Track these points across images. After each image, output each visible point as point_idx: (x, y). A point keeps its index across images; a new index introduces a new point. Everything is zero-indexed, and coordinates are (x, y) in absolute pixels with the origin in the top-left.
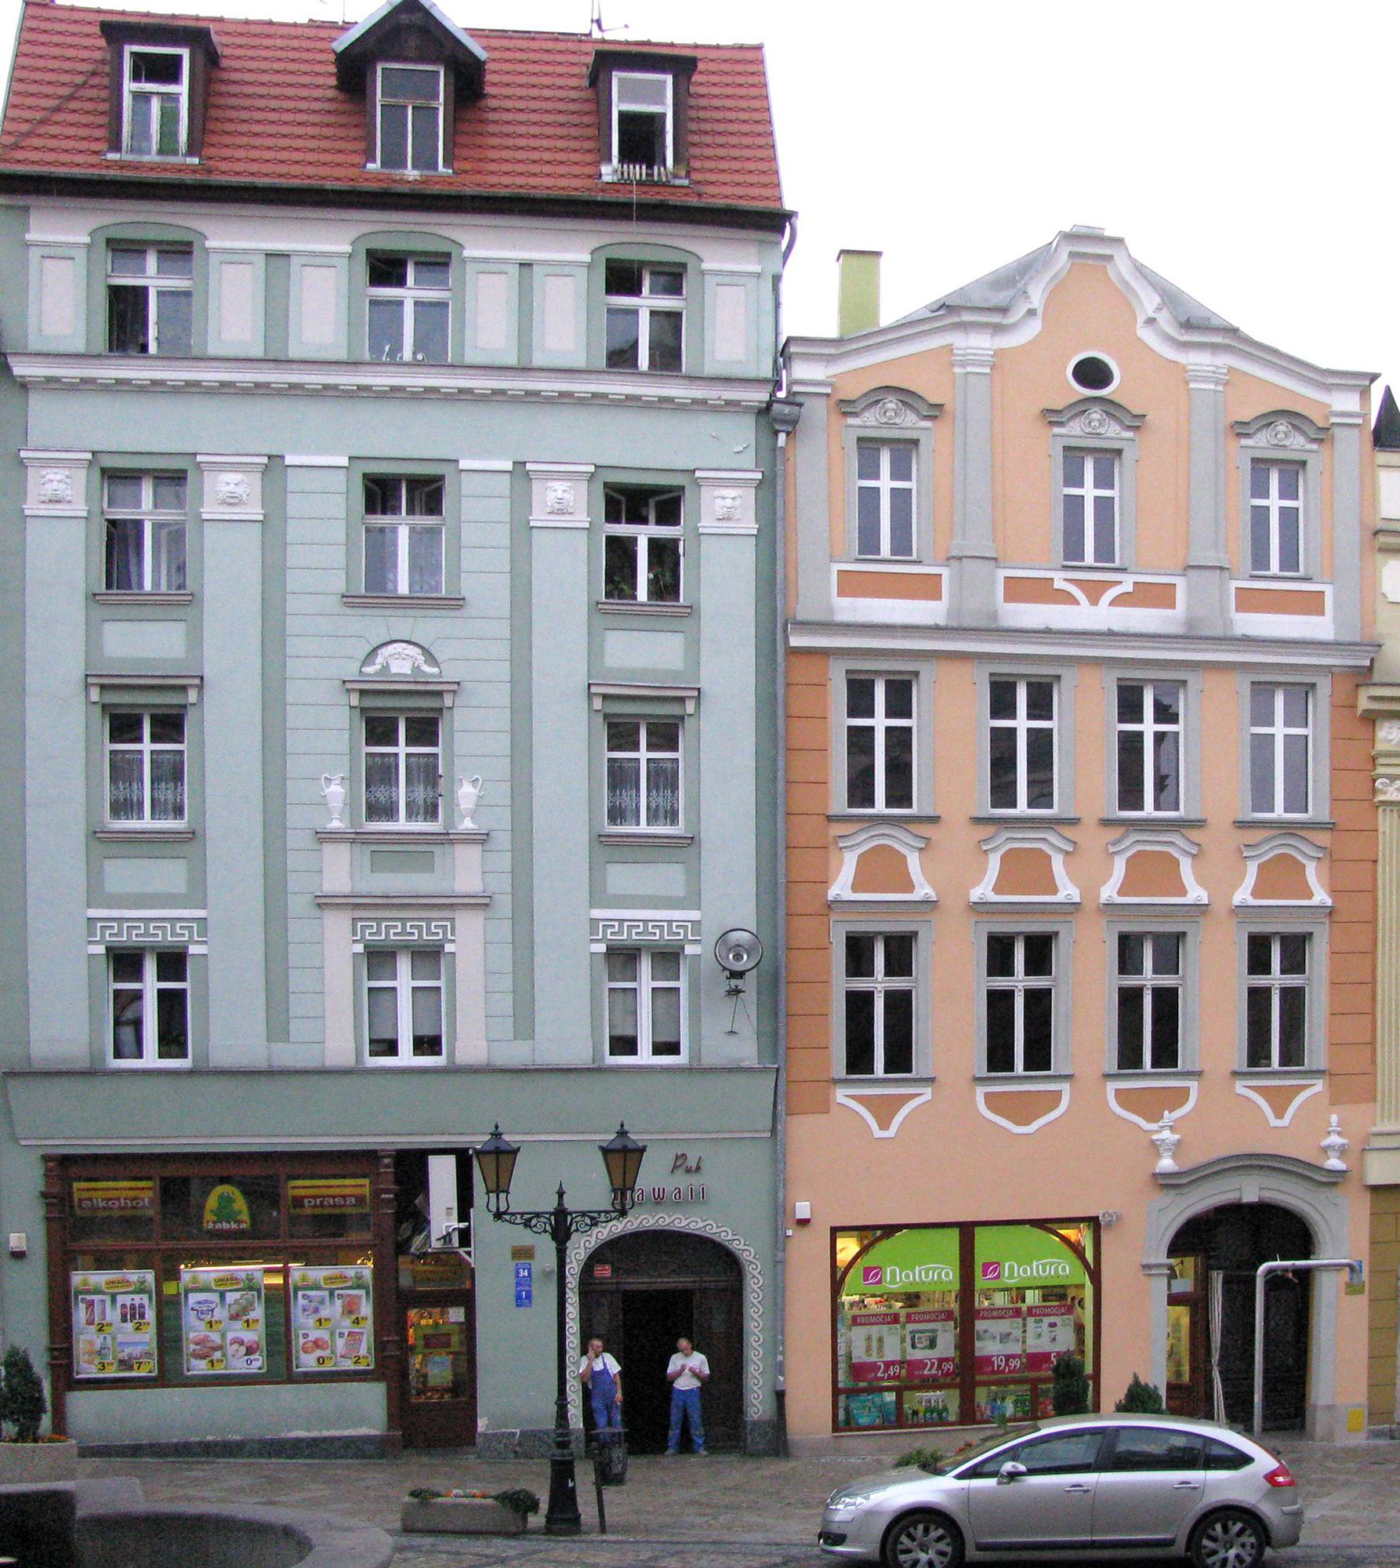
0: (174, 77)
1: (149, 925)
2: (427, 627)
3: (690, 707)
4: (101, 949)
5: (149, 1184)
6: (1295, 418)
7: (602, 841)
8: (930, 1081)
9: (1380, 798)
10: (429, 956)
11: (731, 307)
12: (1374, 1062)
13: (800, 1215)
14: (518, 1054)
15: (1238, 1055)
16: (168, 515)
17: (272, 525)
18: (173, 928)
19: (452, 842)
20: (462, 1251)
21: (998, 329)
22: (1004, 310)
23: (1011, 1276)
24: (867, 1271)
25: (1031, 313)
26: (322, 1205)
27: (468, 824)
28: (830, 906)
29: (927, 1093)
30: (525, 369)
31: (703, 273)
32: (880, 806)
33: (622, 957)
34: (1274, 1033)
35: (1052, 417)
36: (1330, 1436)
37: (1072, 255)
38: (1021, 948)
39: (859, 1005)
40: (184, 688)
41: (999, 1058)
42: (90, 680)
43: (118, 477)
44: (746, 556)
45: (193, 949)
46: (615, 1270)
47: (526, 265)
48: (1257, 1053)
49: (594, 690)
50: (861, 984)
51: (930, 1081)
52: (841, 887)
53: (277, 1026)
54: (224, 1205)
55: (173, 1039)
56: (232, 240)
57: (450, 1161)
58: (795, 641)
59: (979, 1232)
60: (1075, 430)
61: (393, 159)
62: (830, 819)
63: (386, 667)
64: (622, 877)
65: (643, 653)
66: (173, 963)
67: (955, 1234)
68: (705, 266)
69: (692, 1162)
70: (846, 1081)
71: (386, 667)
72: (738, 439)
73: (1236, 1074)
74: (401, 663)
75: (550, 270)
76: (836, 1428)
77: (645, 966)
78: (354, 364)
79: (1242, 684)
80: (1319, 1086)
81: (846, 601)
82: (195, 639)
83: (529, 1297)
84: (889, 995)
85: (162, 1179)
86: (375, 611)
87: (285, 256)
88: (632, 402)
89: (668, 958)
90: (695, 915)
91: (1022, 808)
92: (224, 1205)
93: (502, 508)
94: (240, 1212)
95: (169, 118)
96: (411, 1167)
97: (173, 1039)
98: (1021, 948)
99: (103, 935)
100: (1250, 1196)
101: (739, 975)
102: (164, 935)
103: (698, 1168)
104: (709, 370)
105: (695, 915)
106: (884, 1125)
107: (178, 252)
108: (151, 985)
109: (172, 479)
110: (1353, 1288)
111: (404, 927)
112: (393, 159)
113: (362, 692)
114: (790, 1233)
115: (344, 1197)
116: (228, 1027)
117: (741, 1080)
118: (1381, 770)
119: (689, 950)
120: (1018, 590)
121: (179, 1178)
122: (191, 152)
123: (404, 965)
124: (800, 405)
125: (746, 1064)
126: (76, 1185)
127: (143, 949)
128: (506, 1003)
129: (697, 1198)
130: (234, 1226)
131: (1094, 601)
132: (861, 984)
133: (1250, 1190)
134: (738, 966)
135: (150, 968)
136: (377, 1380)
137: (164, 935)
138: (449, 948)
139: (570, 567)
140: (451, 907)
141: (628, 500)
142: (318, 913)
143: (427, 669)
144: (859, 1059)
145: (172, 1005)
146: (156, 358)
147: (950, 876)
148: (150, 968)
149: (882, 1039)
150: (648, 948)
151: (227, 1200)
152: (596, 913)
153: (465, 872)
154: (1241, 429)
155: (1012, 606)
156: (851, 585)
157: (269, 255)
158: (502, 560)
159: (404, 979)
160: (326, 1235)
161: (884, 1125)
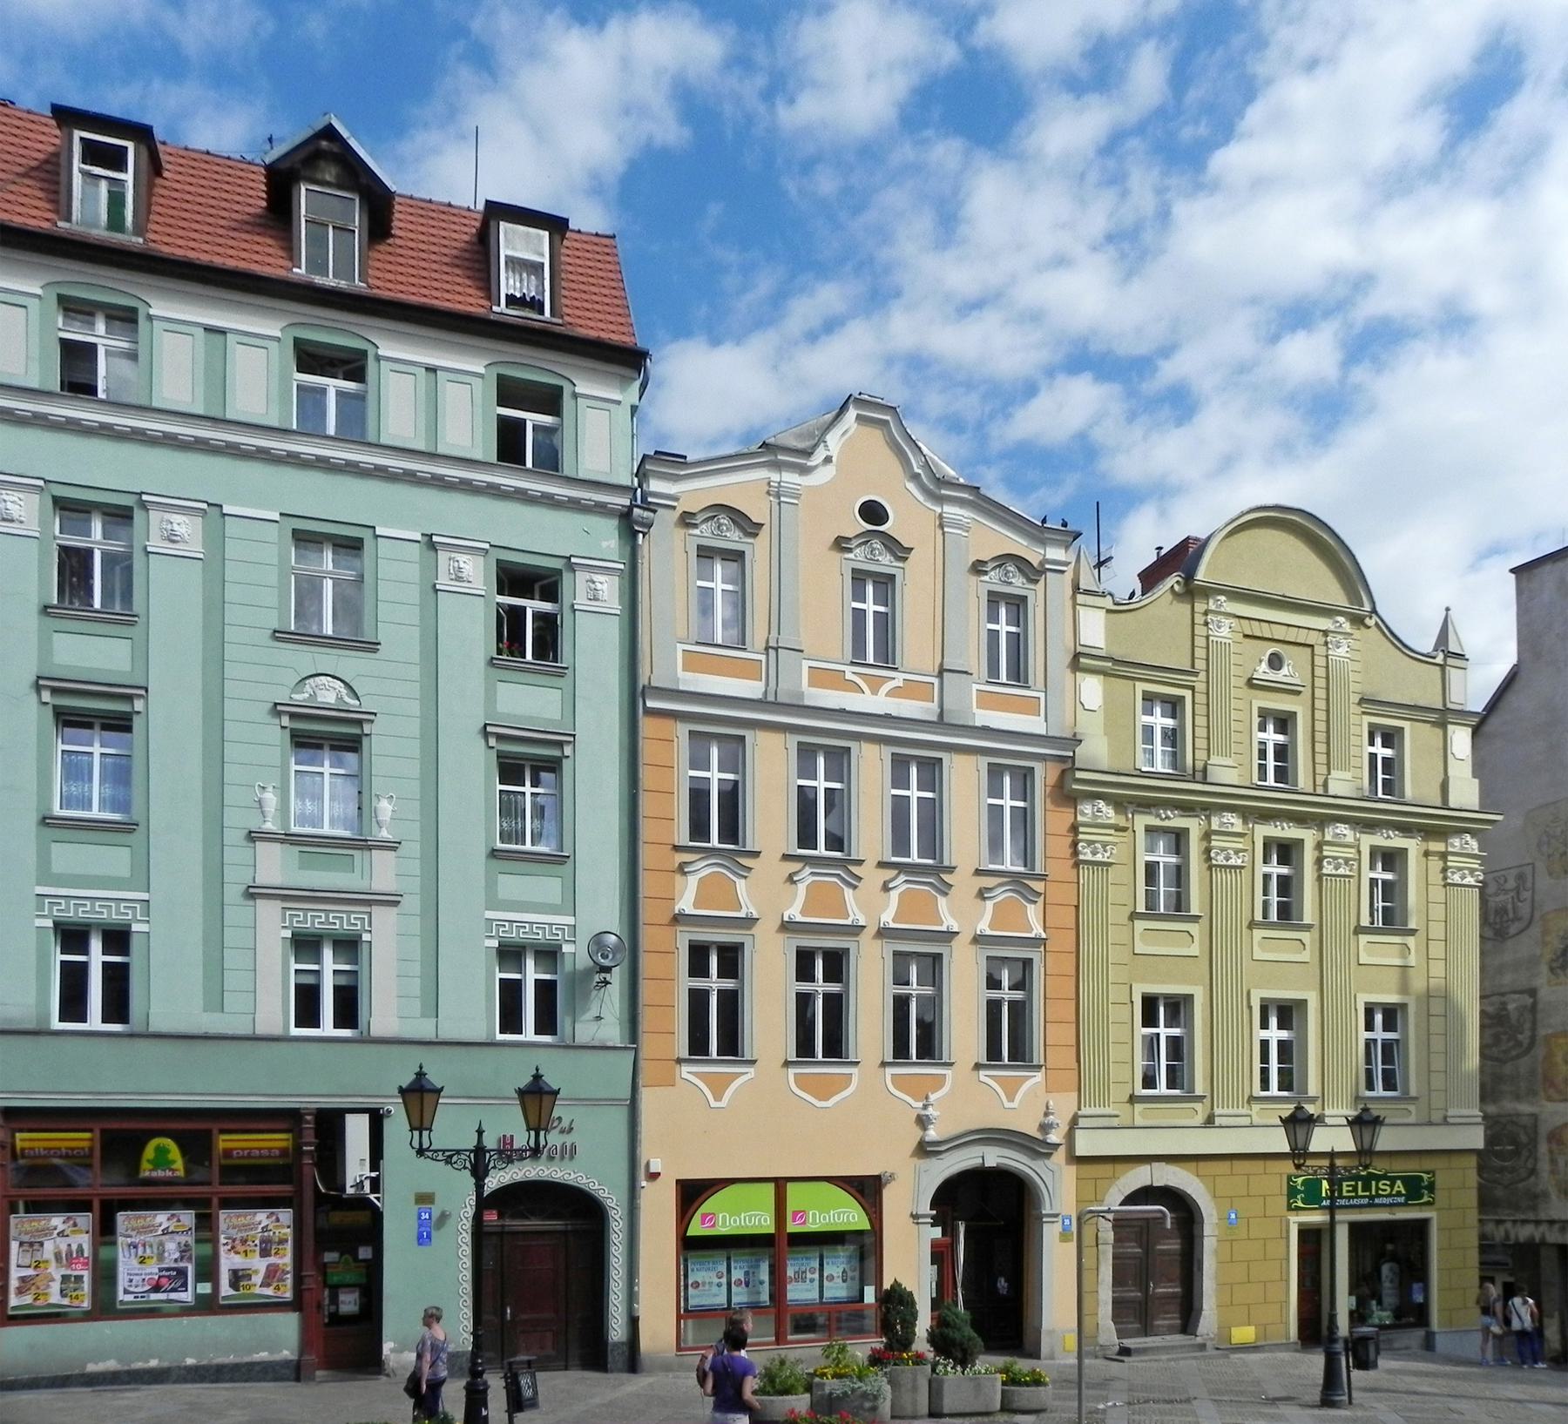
0: (120, 165)
1: (97, 905)
2: (350, 664)
3: (568, 750)
4: (49, 923)
5: (87, 1135)
6: (1021, 563)
7: (494, 854)
8: (753, 1062)
9: (1081, 857)
10: (349, 946)
11: (600, 429)
12: (1079, 1061)
13: (652, 1170)
14: (425, 1030)
15: (979, 1051)
16: (116, 546)
17: (214, 562)
18: (118, 908)
19: (370, 848)
20: (372, 1197)
21: (805, 470)
22: (808, 453)
23: (814, 1222)
24: (704, 1216)
25: (828, 460)
26: (249, 1156)
27: (384, 834)
28: (679, 919)
29: (751, 1070)
30: (433, 456)
31: (575, 396)
32: (715, 841)
33: (510, 954)
34: (1009, 1039)
35: (841, 544)
36: (1052, 1357)
37: (859, 417)
38: (823, 962)
39: (698, 1000)
40: (129, 698)
41: (805, 1047)
42: (41, 682)
43: (71, 509)
44: (613, 632)
45: (135, 927)
46: (501, 1216)
47: (432, 370)
48: (993, 1052)
49: (489, 729)
50: (699, 983)
51: (753, 1062)
52: (686, 904)
53: (216, 999)
54: (164, 1157)
55: (117, 1007)
56: (174, 315)
57: (364, 1119)
58: (650, 704)
59: (790, 1186)
60: (859, 557)
61: (318, 265)
62: (677, 848)
63: (313, 696)
64: (513, 885)
65: (529, 702)
66: (117, 939)
67: (771, 1187)
68: (577, 390)
69: (565, 1124)
70: (685, 1061)
71: (313, 696)
72: (605, 538)
73: (978, 1066)
74: (329, 694)
75: (452, 376)
76: (679, 1348)
77: (530, 963)
78: (284, 432)
79: (983, 762)
80: (1039, 1077)
81: (689, 675)
82: (142, 655)
83: (429, 1237)
84: (722, 993)
85: (103, 1131)
86: (305, 648)
87: (222, 332)
88: (521, 496)
89: (549, 955)
90: (570, 920)
91: (821, 850)
92: (164, 1157)
93: (413, 572)
94: (174, 1162)
95: (116, 201)
96: (330, 1124)
97: (117, 1007)
98: (823, 962)
99: (51, 910)
100: (991, 1162)
101: (607, 970)
102: (110, 913)
103: (571, 1129)
104: (581, 476)
105: (570, 920)
106: (718, 1098)
107: (124, 318)
108: (96, 957)
109: (119, 516)
110: (1064, 1236)
111: (327, 917)
112: (318, 265)
113: (293, 716)
114: (644, 1183)
115: (270, 1149)
116: (166, 997)
117: (610, 1055)
118: (1081, 837)
119: (566, 948)
120: (821, 678)
121: (123, 1132)
122: (139, 230)
123: (328, 953)
124: (654, 512)
125: (610, 1044)
126: (18, 1135)
127: (88, 925)
128: (415, 986)
129: (569, 1153)
130: (169, 1174)
131: (875, 692)
132: (699, 983)
133: (993, 1157)
134: (605, 962)
135: (96, 945)
136: (295, 1310)
137: (110, 913)
138: (366, 937)
139: (470, 624)
140: (369, 903)
141: (517, 579)
142: (251, 903)
143: (347, 699)
144: (698, 1045)
145: (117, 978)
146: (102, 401)
147: (770, 897)
148: (96, 945)
149: (718, 1031)
150: (532, 946)
151: (161, 1151)
152: (490, 914)
153: (382, 873)
154: (978, 568)
155: (813, 690)
156: (693, 663)
157: (209, 330)
158: (413, 614)
159: (330, 965)
160: (257, 1183)
161: (718, 1098)
